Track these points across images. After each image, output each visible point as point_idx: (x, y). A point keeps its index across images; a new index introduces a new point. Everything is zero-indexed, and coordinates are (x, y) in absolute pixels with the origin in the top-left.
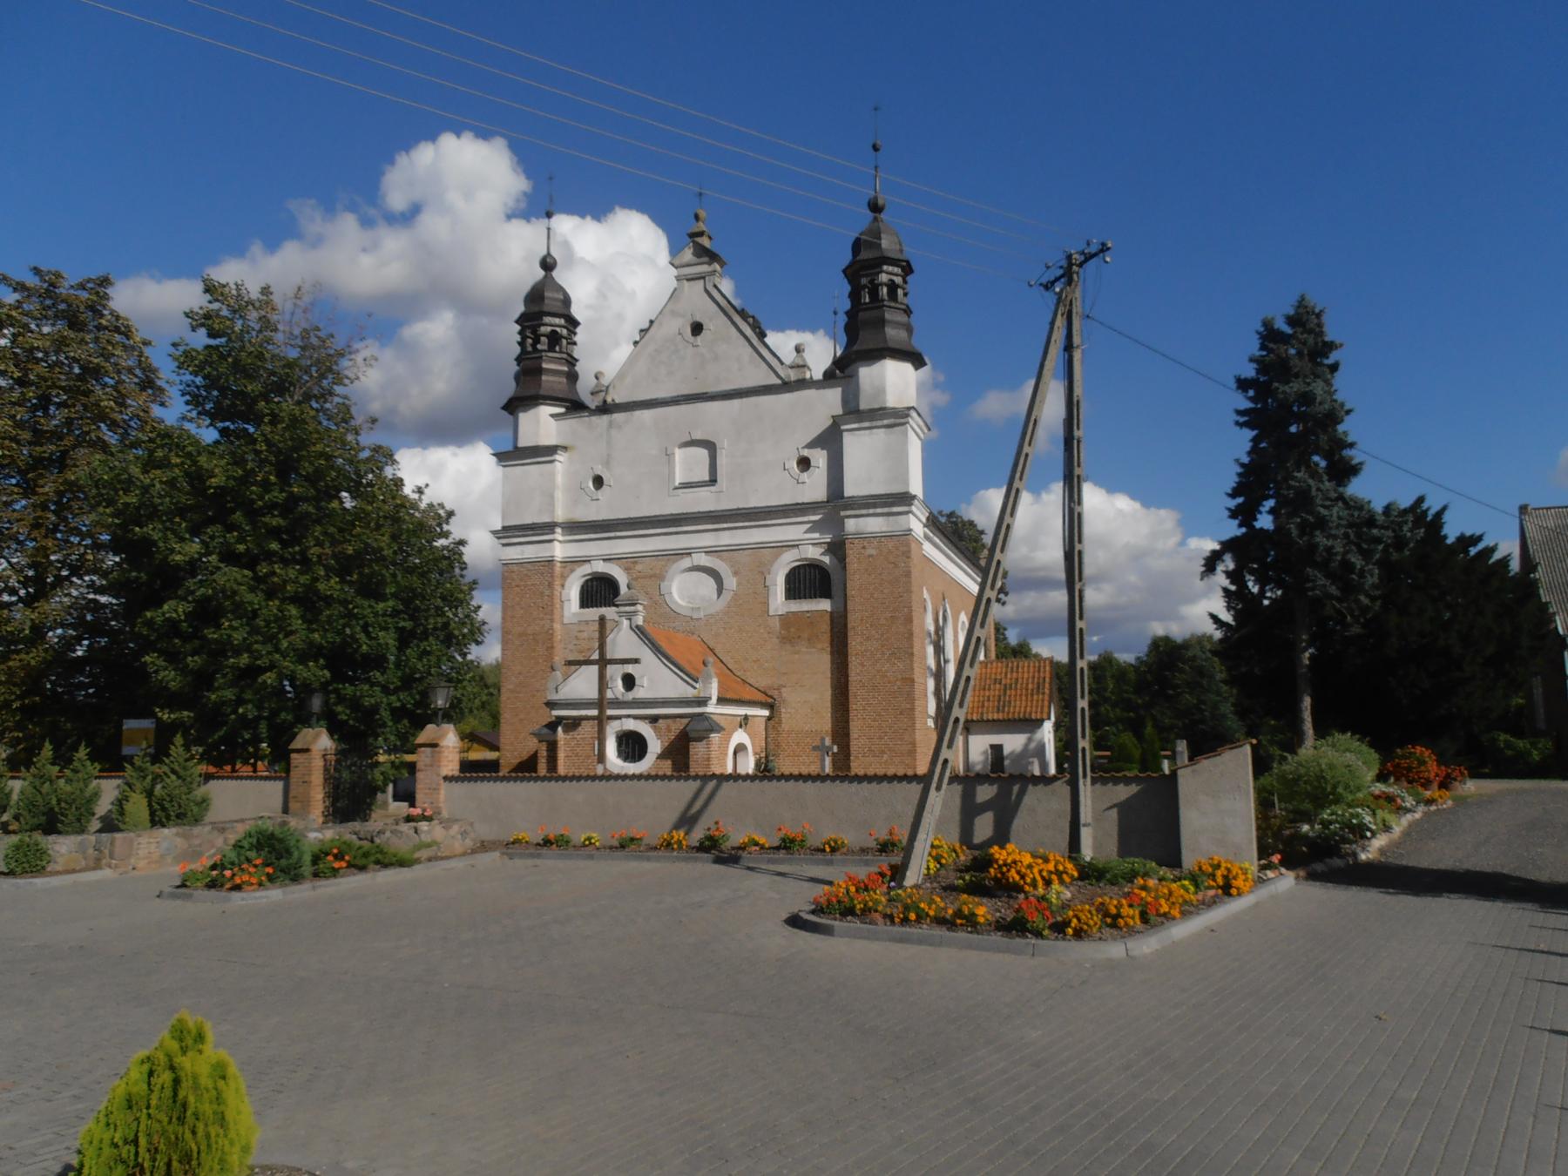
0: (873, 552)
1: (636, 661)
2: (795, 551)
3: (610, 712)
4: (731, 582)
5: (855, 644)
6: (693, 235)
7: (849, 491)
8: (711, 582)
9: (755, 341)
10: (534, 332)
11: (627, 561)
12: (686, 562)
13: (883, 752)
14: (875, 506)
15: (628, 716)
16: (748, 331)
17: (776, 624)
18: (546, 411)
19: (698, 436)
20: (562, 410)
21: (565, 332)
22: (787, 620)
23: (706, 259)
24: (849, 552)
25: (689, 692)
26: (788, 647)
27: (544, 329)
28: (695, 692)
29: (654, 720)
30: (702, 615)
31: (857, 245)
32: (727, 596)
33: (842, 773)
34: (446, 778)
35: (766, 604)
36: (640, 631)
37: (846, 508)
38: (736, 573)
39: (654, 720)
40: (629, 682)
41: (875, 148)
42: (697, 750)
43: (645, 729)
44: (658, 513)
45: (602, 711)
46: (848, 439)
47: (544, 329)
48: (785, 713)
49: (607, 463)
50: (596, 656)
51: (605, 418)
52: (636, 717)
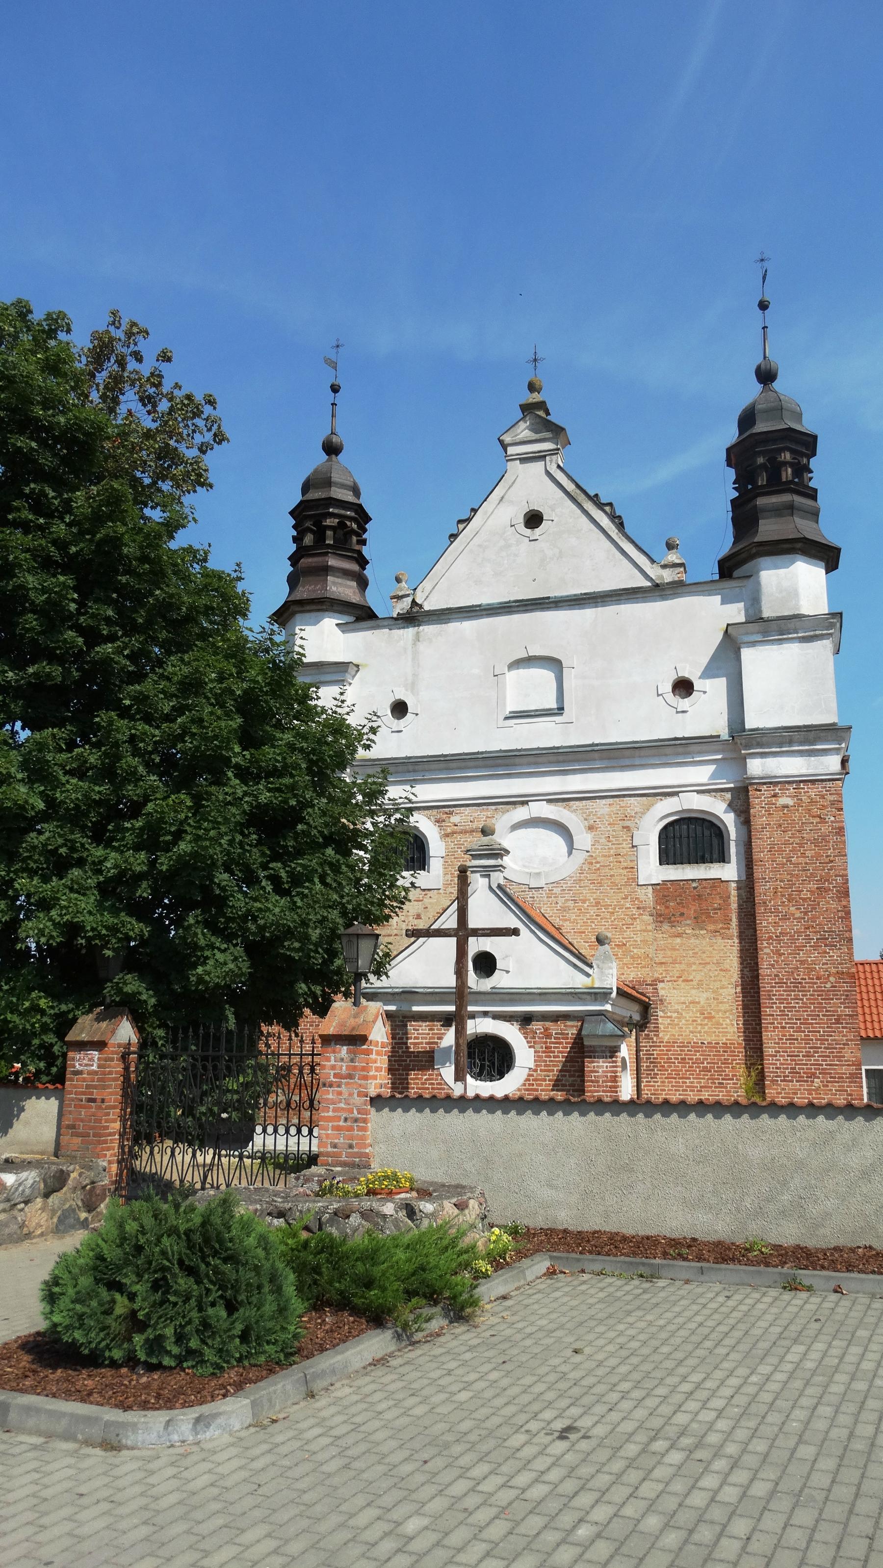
0: (790, 802)
1: (515, 932)
2: (675, 799)
3: (470, 1008)
4: (583, 840)
5: (766, 924)
6: (527, 409)
7: (752, 722)
8: (557, 841)
9: (613, 531)
10: (318, 523)
11: (441, 810)
12: (520, 814)
13: (813, 1075)
14: (791, 743)
15: (485, 1014)
16: (605, 521)
17: (648, 896)
18: (329, 623)
19: (535, 651)
20: (352, 619)
21: (355, 526)
22: (663, 890)
23: (548, 435)
24: (754, 801)
25: (579, 981)
26: (666, 927)
27: (329, 522)
28: (587, 982)
29: (525, 1020)
30: (541, 883)
31: (747, 419)
32: (579, 858)
33: (757, 1104)
34: (377, 1101)
35: (633, 869)
36: (503, 893)
37: (747, 747)
38: (591, 828)
39: (525, 1020)
40: (486, 964)
41: (763, 306)
42: (598, 1067)
43: (510, 1033)
44: (482, 749)
45: (461, 1006)
46: (747, 654)
47: (329, 522)
48: (662, 1018)
49: (412, 686)
50: (450, 921)
51: (410, 632)
52: (496, 1016)
